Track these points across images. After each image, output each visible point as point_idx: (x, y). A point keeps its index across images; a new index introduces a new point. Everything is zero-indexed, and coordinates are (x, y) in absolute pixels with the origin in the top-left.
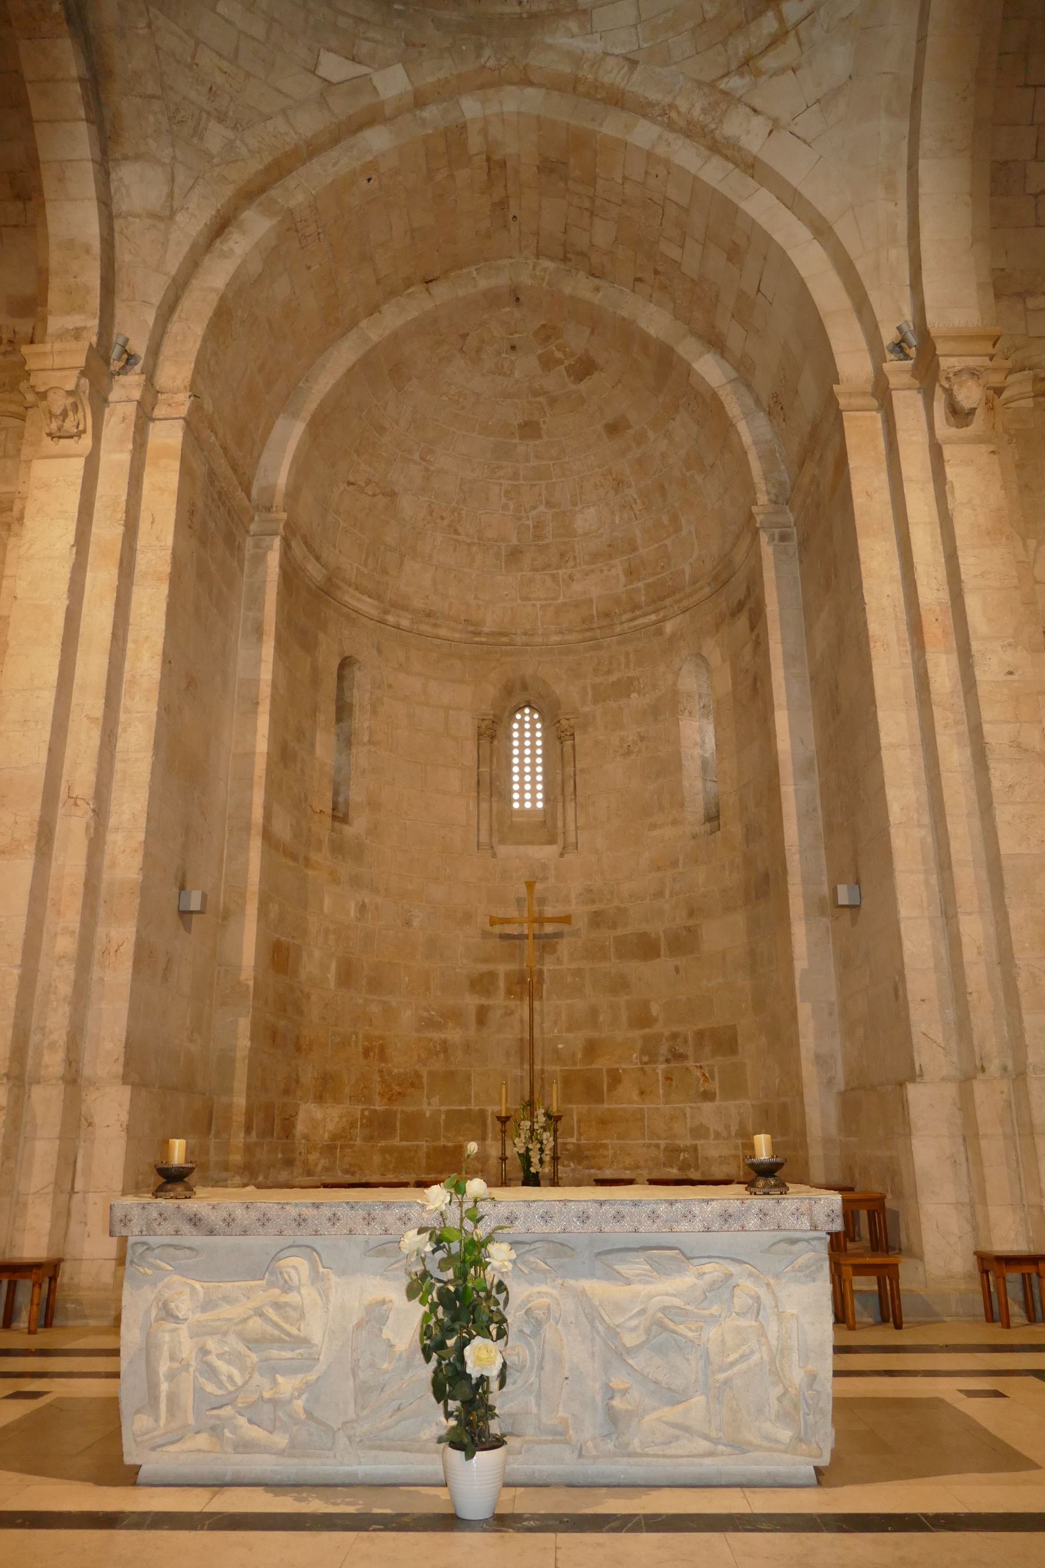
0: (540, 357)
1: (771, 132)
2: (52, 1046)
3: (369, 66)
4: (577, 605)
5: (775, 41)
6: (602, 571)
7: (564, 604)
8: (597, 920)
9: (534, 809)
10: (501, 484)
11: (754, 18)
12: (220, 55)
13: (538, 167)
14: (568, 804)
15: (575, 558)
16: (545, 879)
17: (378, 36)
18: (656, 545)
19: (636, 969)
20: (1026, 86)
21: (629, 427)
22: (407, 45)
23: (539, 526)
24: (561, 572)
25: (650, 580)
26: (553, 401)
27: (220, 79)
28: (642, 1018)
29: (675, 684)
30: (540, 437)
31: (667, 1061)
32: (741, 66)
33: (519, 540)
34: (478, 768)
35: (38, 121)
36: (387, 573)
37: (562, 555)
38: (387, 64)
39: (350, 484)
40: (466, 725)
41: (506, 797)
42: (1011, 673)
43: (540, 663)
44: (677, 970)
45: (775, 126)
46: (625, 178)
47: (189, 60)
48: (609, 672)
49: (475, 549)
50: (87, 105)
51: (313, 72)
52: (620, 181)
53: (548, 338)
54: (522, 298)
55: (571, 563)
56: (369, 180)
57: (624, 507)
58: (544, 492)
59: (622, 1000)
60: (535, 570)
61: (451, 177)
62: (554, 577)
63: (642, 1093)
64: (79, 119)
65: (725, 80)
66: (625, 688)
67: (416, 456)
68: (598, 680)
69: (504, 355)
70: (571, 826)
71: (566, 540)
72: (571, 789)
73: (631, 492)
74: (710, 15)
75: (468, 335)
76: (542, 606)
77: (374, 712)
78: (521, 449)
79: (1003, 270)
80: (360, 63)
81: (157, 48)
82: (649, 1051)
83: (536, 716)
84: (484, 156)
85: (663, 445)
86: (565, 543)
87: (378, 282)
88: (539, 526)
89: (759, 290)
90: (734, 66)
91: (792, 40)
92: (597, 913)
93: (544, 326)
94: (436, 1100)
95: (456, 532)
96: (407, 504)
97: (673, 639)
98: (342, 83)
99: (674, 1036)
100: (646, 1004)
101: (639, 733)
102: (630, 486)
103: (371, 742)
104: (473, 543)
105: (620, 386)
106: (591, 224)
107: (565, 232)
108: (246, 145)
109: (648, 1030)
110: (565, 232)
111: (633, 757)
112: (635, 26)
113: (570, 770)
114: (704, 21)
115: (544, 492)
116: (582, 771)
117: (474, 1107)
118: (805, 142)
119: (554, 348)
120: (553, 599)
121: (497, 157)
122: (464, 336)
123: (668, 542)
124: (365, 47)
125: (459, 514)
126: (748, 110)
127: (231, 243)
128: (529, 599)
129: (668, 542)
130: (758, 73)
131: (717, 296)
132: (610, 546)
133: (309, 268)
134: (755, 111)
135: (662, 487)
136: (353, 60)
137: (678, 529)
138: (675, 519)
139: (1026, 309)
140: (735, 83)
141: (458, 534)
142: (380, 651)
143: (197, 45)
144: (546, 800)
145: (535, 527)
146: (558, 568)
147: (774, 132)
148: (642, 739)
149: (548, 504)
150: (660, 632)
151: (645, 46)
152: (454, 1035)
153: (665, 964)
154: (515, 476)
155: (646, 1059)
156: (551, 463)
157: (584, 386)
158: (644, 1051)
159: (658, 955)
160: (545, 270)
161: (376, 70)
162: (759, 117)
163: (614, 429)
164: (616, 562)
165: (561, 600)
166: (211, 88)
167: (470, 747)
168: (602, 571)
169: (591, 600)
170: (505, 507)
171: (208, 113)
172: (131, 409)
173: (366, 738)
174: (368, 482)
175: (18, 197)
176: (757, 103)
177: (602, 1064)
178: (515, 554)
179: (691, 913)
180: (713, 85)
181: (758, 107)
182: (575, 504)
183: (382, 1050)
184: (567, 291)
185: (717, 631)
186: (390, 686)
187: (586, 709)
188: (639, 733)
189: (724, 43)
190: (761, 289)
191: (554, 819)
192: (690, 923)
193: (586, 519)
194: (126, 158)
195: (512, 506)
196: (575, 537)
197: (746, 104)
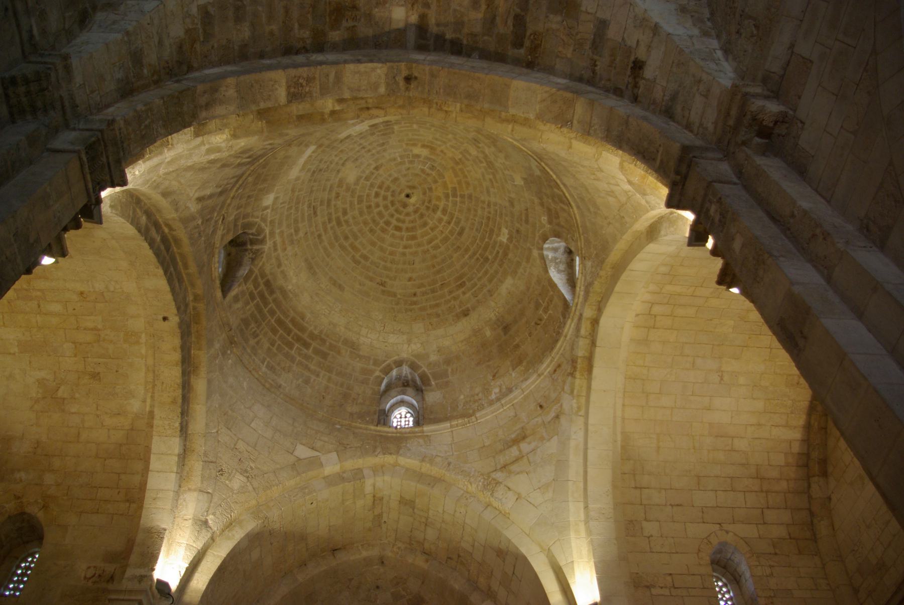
1: (517, 499)
3: (319, 452)
5: (517, 460)
11: (508, 448)
12: (248, 444)
13: (400, 501)
17: (326, 439)
20: (636, 488)
22: (340, 444)
32: (502, 468)
35: (151, 471)
38: (330, 452)
45: (519, 497)
46: (444, 511)
47: (233, 446)
50: (178, 466)
51: (292, 454)
52: (442, 512)
54: (385, 562)
56: (312, 503)
61: (355, 503)
64: (172, 472)
65: (494, 473)
69: (372, 591)
74: (486, 444)
75: (353, 579)
79: (637, 573)
80: (316, 450)
84: (372, 495)
87: (307, 549)
89: (513, 573)
90: (499, 467)
91: (525, 459)
93: (396, 577)
98: (304, 459)
106: (425, 530)
107: (411, 532)
110: (411, 532)
112: (451, 444)
114: (484, 446)
118: (534, 505)
119: (401, 589)
121: (378, 496)
122: (350, 580)
124: (319, 444)
127: (234, 532)
130: (510, 472)
131: (492, 572)
133: (271, 544)
134: (509, 488)
136: (313, 449)
139: (652, 594)
140: (499, 476)
143: (238, 440)
147: (518, 500)
151: (455, 453)
160: (399, 548)
161: (323, 454)
162: (511, 492)
166: (240, 459)
171: (236, 470)
175: (128, 501)
176: (510, 485)
180: (489, 475)
184: (410, 561)
190: (515, 572)
194: (189, 490)
197: (505, 486)
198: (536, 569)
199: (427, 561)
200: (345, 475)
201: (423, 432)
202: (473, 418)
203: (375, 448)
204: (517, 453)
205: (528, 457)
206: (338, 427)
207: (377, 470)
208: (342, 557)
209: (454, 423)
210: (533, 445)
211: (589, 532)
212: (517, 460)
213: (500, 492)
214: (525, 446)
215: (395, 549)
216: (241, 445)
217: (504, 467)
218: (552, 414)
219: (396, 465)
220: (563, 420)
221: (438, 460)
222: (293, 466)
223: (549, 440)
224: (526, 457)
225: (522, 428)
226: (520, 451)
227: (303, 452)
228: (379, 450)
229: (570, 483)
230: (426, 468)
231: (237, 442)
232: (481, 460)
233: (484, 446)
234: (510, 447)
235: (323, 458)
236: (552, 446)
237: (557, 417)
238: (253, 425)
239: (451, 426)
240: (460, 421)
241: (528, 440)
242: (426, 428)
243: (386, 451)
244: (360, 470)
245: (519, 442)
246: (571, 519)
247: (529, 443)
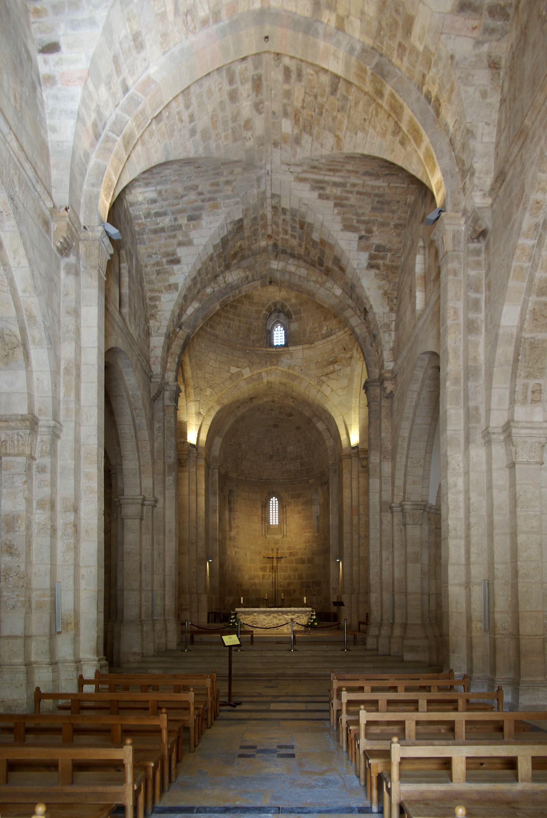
5: (333, 372)
8: (291, 554)
9: (276, 524)
16: (278, 544)
17: (243, 361)
38: (246, 367)
41: (269, 522)
74: (319, 361)
92: (291, 553)
130: (329, 378)
144: (279, 522)
172: (194, 458)
191: (281, 528)
198: (337, 424)
199: (294, 402)
200: (254, 377)
201: (289, 351)
202: (313, 345)
203: (266, 362)
204: (333, 369)
206: (248, 351)
207: (267, 373)
208: (255, 402)
209: (304, 346)
210: (340, 367)
211: (359, 414)
215: (279, 396)
217: (327, 374)
218: (348, 356)
219: (276, 369)
220: (353, 360)
221: (297, 367)
226: (334, 368)
227: (234, 370)
228: (268, 364)
229: (354, 390)
230: (291, 371)
235: (243, 371)
236: (348, 370)
237: (351, 358)
239: (303, 349)
240: (307, 346)
241: (338, 363)
242: (291, 348)
243: (272, 364)
244: (260, 373)
246: (353, 405)
247: (338, 366)
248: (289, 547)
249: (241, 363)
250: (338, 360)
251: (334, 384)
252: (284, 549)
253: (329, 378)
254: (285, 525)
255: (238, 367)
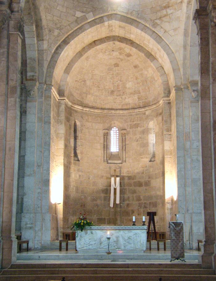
0: (119, 53)
2: (39, 207)
4: (127, 105)
5: (165, 16)
6: (132, 97)
7: (124, 104)
10: (109, 76)
14: (124, 151)
15: (126, 94)
17: (87, 6)
18: (145, 93)
19: (138, 189)
21: (139, 67)
23: (118, 86)
24: (123, 97)
25: (144, 101)
26: (122, 60)
27: (57, 21)
28: (139, 199)
29: (148, 126)
30: (119, 66)
31: (144, 208)
33: (114, 89)
34: (104, 143)
36: (83, 99)
37: (123, 93)
38: (89, 12)
39: (76, 81)
40: (101, 133)
42: (198, 147)
43: (118, 118)
44: (146, 189)
48: (133, 122)
49: (103, 91)
51: (75, 16)
53: (121, 50)
55: (125, 95)
57: (138, 83)
58: (119, 78)
59: (135, 195)
60: (117, 96)
62: (121, 98)
63: (138, 215)
66: (137, 126)
67: (90, 72)
68: (131, 123)
70: (124, 157)
71: (125, 89)
72: (125, 148)
73: (139, 80)
76: (119, 105)
77: (81, 132)
78: (114, 69)
81: (47, 20)
82: (140, 205)
83: (117, 129)
85: (146, 73)
86: (124, 90)
88: (118, 86)
90: (158, 18)
91: (168, 17)
93: (120, 48)
94: (95, 216)
95: (99, 87)
96: (88, 83)
97: (147, 116)
99: (145, 203)
100: (139, 196)
101: (140, 137)
102: (139, 79)
103: (81, 139)
104: (103, 90)
105: (137, 60)
108: (62, 32)
109: (140, 202)
111: (138, 142)
113: (124, 144)
114: (153, 7)
115: (119, 78)
116: (127, 144)
117: (103, 217)
118: (171, 35)
120: (121, 103)
123: (147, 93)
125: (100, 83)
126: (160, 27)
128: (115, 103)
129: (147, 93)
130: (163, 21)
132: (134, 92)
134: (162, 27)
135: (146, 81)
137: (149, 91)
138: (149, 88)
141: (99, 88)
142: (82, 118)
145: (117, 86)
146: (123, 95)
148: (141, 138)
149: (120, 81)
150: (145, 114)
152: (99, 202)
153: (144, 188)
154: (113, 74)
155: (139, 208)
156: (121, 72)
157: (129, 58)
158: (139, 206)
159: (142, 186)
163: (136, 67)
164: (136, 95)
165: (123, 103)
167: (102, 138)
168: (132, 97)
169: (130, 104)
170: (110, 81)
173: (80, 138)
174: (80, 79)
176: (162, 26)
177: (130, 209)
178: (112, 92)
179: (149, 178)
180: (154, 20)
181: (163, 27)
182: (126, 81)
183: (84, 205)
185: (156, 117)
186: (84, 126)
187: (128, 130)
188: (140, 137)
189: (156, 13)
192: (149, 180)
193: (129, 85)
194: (40, 40)
195: (112, 81)
196: (126, 88)
205: (169, 16)
210: (172, 11)
212: (165, 16)
213: (158, 28)
214: (169, 11)
216: (55, 18)
222: (76, 21)
223: (178, 11)
224: (169, 16)
225: (168, 2)
226: (167, 12)
227: (79, 14)
231: (53, 17)
232: (151, 13)
233: (153, 7)
234: (162, 10)
235: (87, 16)
238: (58, 9)
241: (170, 8)
245: (167, 8)
247: (171, 10)
248: (128, 171)
249: (85, 9)
250: (170, 5)
251: (166, 26)
252: (124, 174)
253: (163, 21)
254: (124, 152)
255: (82, 12)
